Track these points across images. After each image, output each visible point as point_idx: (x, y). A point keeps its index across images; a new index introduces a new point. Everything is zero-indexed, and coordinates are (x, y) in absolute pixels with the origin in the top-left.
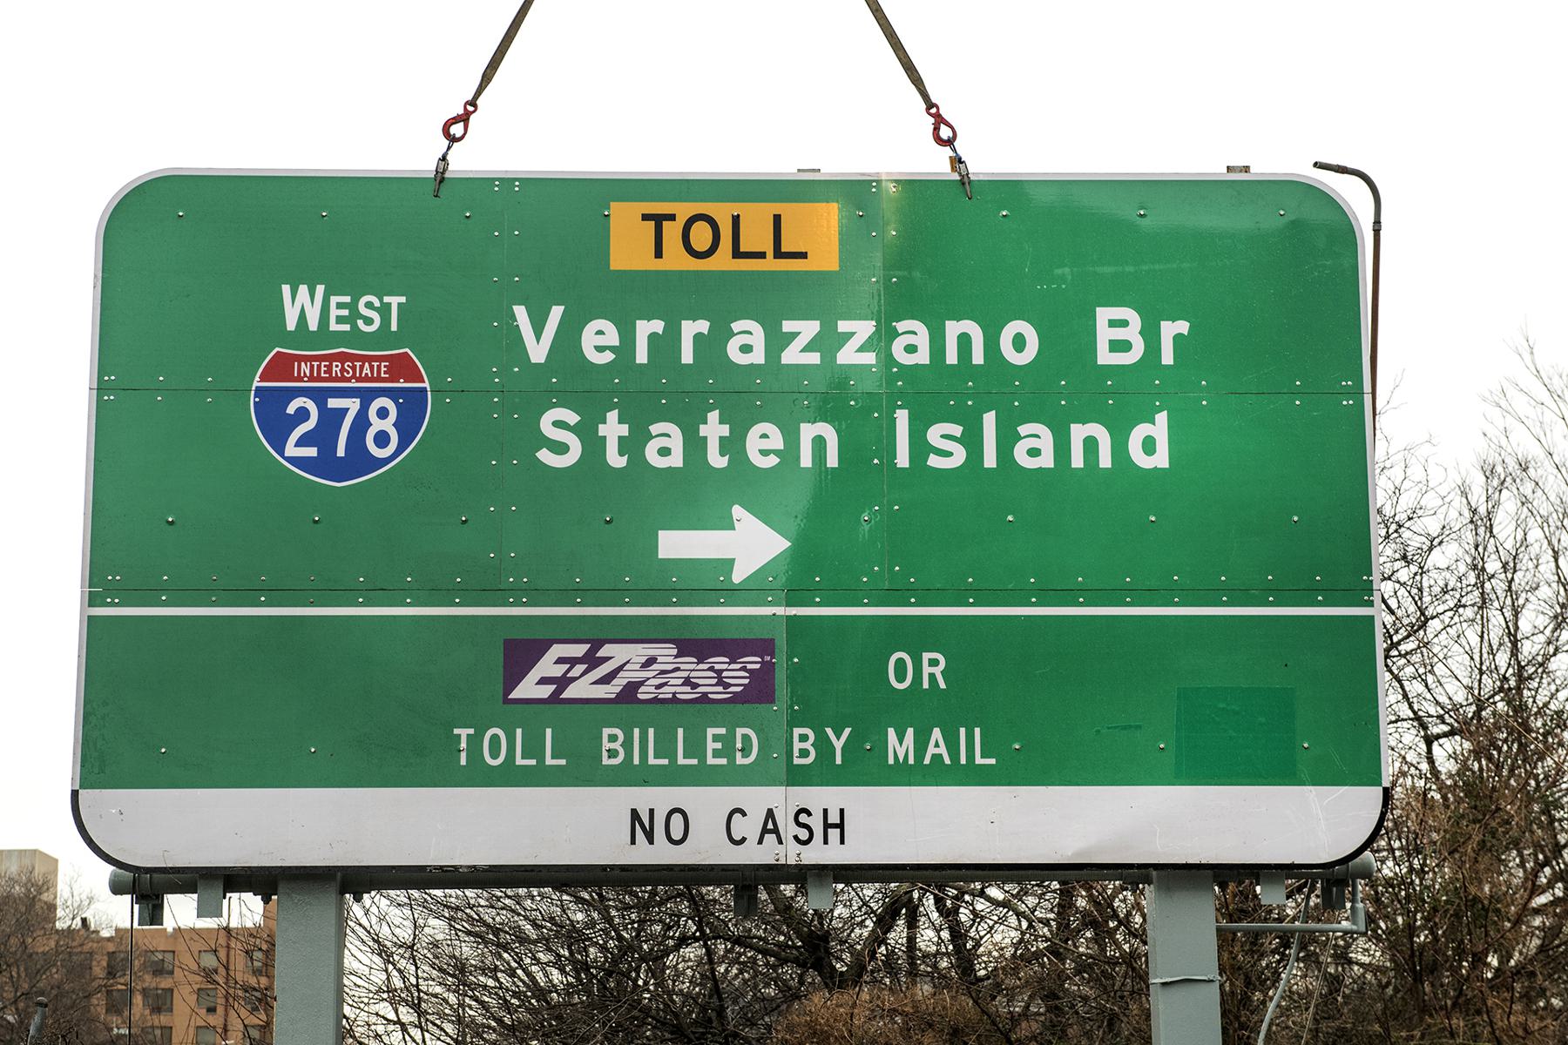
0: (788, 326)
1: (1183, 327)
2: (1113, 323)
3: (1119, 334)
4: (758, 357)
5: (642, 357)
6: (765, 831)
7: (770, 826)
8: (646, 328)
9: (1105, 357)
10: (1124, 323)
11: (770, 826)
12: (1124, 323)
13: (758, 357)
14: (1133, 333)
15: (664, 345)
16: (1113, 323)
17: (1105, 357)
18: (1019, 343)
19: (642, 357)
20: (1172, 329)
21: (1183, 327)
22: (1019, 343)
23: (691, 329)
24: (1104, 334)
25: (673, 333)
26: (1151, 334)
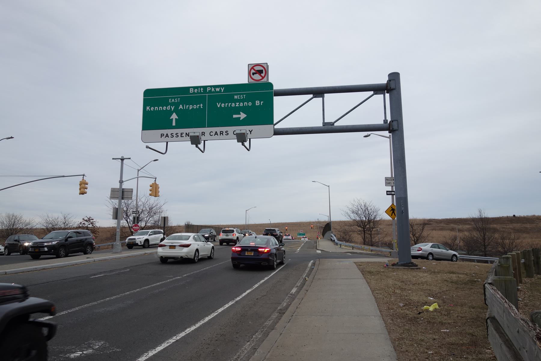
0: (236, 103)
1: (263, 102)
2: (257, 102)
3: (257, 103)
4: (234, 106)
5: (226, 106)
6: (215, 134)
7: (216, 133)
8: (226, 104)
9: (257, 105)
10: (258, 102)
11: (216, 133)
12: (258, 102)
13: (234, 106)
14: (259, 103)
15: (228, 105)
16: (257, 102)
17: (257, 105)
18: (250, 104)
19: (226, 106)
20: (262, 102)
21: (263, 102)
22: (250, 104)
23: (230, 104)
24: (257, 103)
25: (228, 104)
26: (260, 103)
